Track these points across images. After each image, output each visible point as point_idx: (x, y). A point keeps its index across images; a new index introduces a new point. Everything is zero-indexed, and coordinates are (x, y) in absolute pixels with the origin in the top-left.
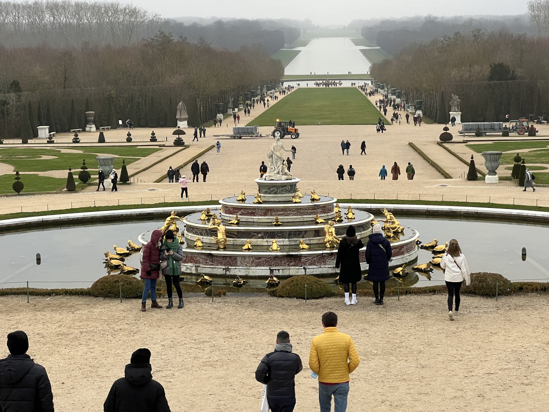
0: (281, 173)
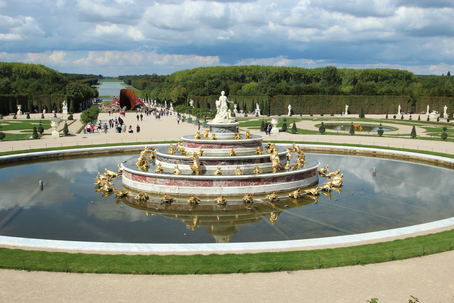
0: (227, 118)
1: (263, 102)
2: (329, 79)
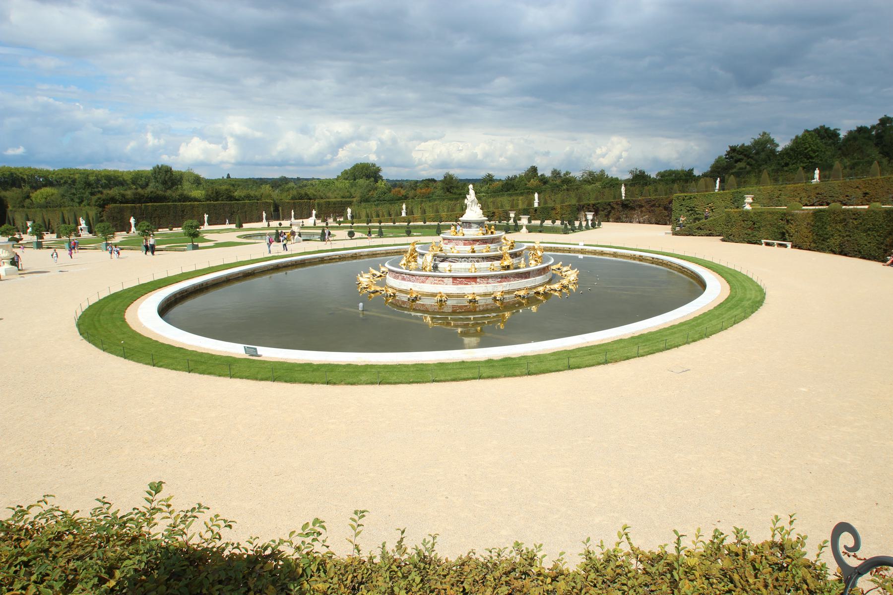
1: (87, 215)
2: (164, 183)
